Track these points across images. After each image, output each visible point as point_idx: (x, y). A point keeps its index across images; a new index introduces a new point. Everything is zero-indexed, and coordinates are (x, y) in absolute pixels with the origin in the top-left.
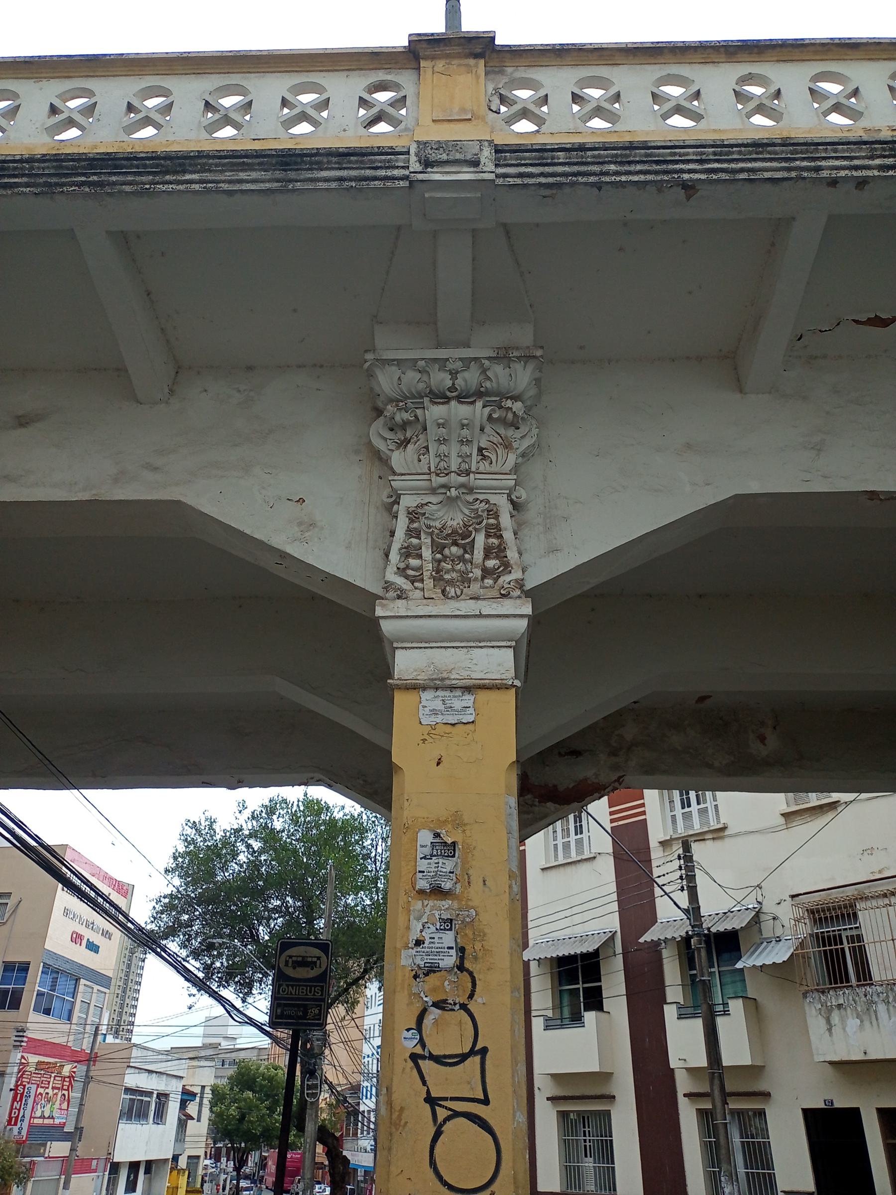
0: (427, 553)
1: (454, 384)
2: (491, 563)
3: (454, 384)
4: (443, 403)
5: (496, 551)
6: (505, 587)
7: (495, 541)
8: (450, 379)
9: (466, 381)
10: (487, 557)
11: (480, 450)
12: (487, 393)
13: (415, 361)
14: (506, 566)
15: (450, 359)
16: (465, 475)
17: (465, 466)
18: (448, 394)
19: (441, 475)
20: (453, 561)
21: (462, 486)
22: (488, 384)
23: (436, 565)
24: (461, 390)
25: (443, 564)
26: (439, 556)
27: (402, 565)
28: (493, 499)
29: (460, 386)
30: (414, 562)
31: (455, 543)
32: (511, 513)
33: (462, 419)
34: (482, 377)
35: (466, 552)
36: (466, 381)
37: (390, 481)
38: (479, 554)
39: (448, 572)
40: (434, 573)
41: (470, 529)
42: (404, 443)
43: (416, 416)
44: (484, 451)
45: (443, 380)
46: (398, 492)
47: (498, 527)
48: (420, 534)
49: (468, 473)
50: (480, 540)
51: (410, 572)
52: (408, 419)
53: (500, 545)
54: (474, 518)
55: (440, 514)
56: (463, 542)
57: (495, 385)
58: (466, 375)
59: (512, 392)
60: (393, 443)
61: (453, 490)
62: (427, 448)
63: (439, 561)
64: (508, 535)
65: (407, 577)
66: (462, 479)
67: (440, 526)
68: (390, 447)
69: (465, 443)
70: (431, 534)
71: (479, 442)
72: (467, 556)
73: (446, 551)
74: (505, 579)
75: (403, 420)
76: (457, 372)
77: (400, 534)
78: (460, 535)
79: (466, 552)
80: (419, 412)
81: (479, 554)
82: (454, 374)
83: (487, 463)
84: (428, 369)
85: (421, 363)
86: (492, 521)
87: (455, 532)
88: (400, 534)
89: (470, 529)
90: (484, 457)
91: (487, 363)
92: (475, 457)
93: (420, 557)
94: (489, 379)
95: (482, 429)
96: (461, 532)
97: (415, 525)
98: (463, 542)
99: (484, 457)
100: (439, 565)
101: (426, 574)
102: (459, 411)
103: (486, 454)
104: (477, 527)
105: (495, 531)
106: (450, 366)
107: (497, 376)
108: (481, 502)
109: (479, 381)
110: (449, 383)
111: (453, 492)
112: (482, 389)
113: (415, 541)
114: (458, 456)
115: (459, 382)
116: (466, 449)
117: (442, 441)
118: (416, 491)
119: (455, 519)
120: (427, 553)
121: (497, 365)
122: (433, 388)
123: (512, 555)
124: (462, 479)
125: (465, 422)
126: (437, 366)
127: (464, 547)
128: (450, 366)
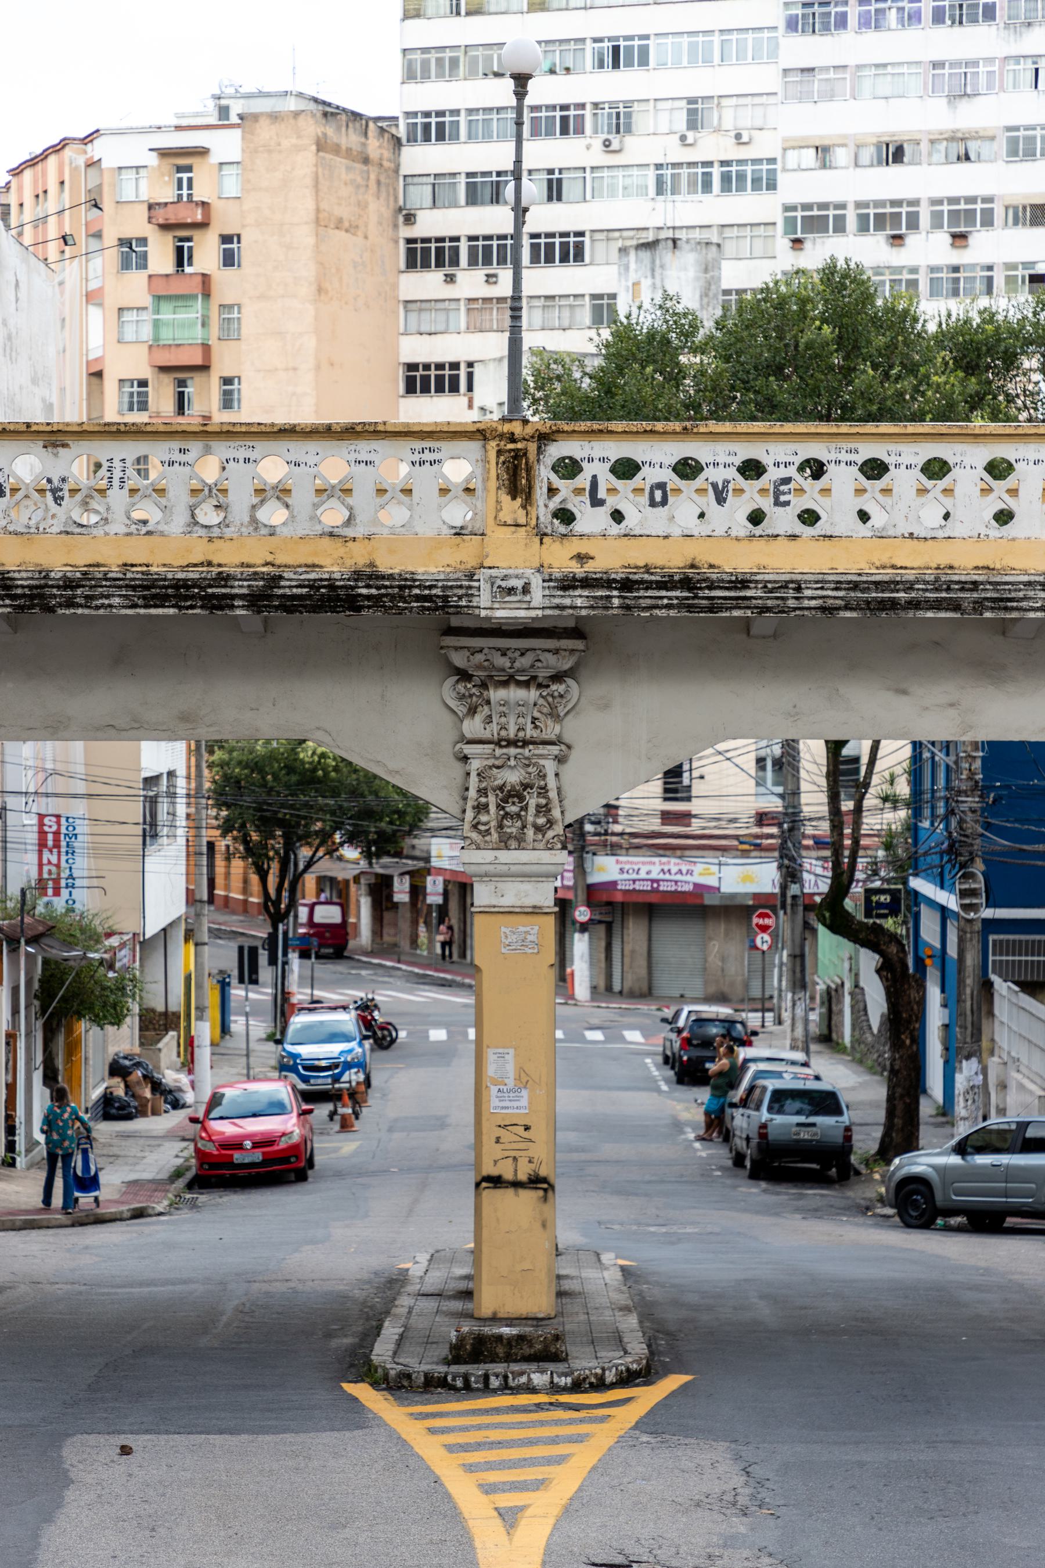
0: (492, 808)
2: (541, 821)
5: (544, 809)
7: (543, 801)
10: (537, 816)
11: (534, 720)
14: (551, 823)
17: (521, 734)
28: (542, 762)
30: (484, 818)
31: (514, 803)
38: (532, 810)
42: (472, 711)
47: (544, 788)
49: (526, 743)
50: (533, 802)
51: (482, 828)
62: (490, 716)
64: (553, 794)
65: (480, 832)
74: (550, 834)
77: (472, 793)
81: (532, 810)
82: (513, 661)
86: (542, 783)
88: (472, 793)
90: (536, 727)
92: (529, 726)
93: (488, 812)
97: (484, 785)
101: (492, 830)
102: (515, 694)
105: (543, 791)
113: (483, 800)
115: (517, 665)
117: (504, 715)
118: (480, 756)
119: (512, 777)
120: (492, 808)
123: (556, 813)
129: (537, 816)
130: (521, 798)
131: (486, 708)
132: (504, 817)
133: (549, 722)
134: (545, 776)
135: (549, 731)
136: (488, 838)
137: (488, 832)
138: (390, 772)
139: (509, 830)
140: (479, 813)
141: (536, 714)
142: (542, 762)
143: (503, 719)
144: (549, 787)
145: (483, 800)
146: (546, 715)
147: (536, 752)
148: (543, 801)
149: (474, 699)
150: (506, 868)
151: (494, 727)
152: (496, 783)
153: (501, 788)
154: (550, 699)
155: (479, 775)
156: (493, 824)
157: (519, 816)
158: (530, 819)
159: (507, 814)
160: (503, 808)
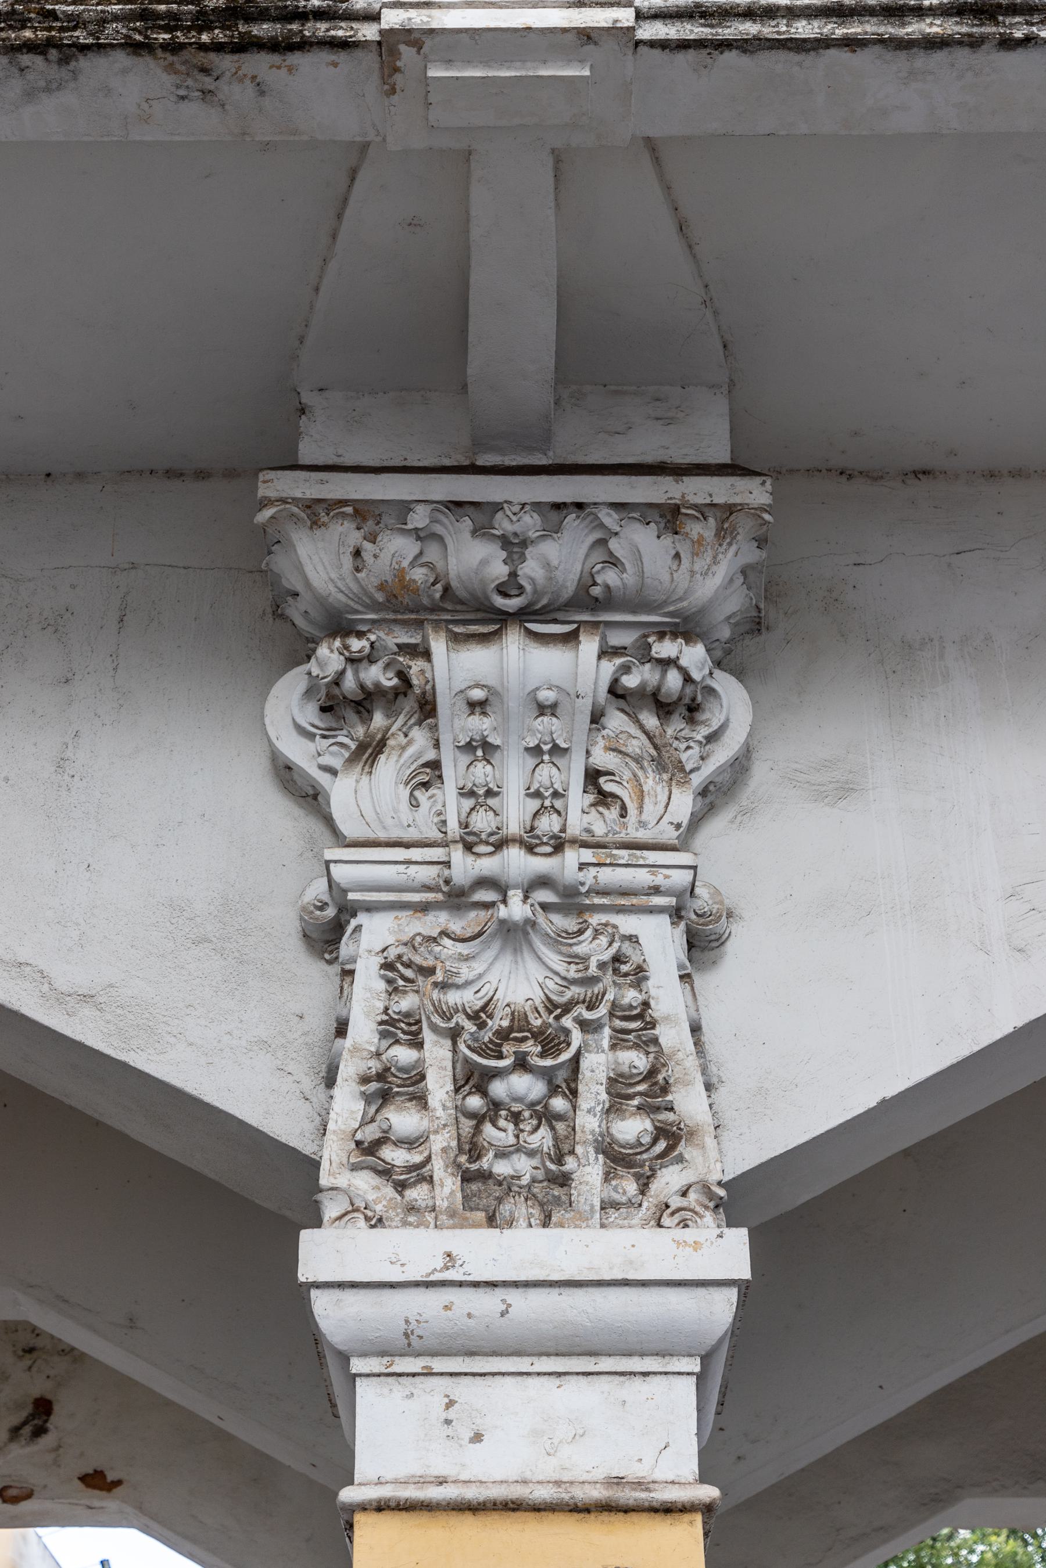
1: (513, 575)
3: (513, 575)
4: (484, 639)
6: (673, 1207)
7: (637, 1060)
8: (505, 562)
9: (547, 565)
10: (615, 1106)
11: (593, 776)
12: (608, 601)
13: (405, 507)
15: (505, 505)
16: (548, 849)
17: (548, 824)
18: (499, 601)
19: (482, 849)
20: (516, 1118)
21: (543, 882)
22: (610, 577)
23: (467, 1125)
24: (535, 591)
25: (488, 1129)
26: (475, 1102)
27: (370, 1133)
29: (532, 580)
31: (522, 1064)
32: (681, 967)
33: (537, 689)
34: (598, 556)
35: (554, 1090)
36: (547, 565)
37: (327, 863)
39: (502, 1154)
40: (463, 1159)
41: (567, 1022)
43: (403, 676)
44: (602, 780)
45: (484, 562)
46: (351, 896)
47: (643, 1013)
48: (420, 1031)
51: (396, 1156)
52: (377, 685)
53: (652, 1072)
54: (574, 982)
55: (478, 967)
56: (548, 1062)
57: (630, 578)
58: (550, 549)
59: (681, 599)
60: (335, 748)
61: (515, 897)
62: (435, 765)
63: (479, 1119)
65: (385, 1172)
66: (540, 865)
67: (480, 1004)
68: (327, 760)
69: (546, 757)
70: (454, 1034)
71: (588, 753)
72: (559, 1104)
73: (498, 1089)
75: (362, 687)
76: (524, 543)
78: (537, 1035)
79: (554, 1090)
80: (416, 667)
83: (612, 814)
84: (438, 529)
85: (419, 518)
86: (631, 996)
87: (519, 1023)
89: (567, 1022)
90: (604, 799)
91: (609, 519)
92: (577, 799)
93: (421, 1100)
94: (613, 562)
95: (597, 718)
96: (538, 1022)
97: (406, 1003)
98: (548, 1062)
99: (604, 799)
100: (477, 1130)
101: (438, 1168)
103: (609, 787)
104: (588, 1015)
106: (503, 524)
107: (638, 556)
108: (597, 933)
109: (588, 566)
110: (499, 570)
111: (516, 909)
112: (596, 591)
113: (403, 1055)
114: (528, 795)
115: (531, 569)
116: (547, 774)
121: (637, 526)
122: (454, 584)
124: (540, 865)
125: (547, 696)
126: (467, 524)
127: (547, 1074)
128: (503, 524)
129: (615, 1106)
130: (551, 1044)
131: (420, 737)
132: (479, 1119)
133: (651, 781)
134: (639, 976)
135: (651, 811)
136: (417, 1194)
137: (420, 1173)
138: (60, 998)
139: (502, 1168)
140: (385, 1097)
141: (602, 759)
142: (627, 924)
143: (481, 773)
144: (658, 1010)
145: (403, 1055)
146: (638, 760)
147: (608, 876)
148: (637, 1060)
149: (379, 720)
150: (487, 1303)
151: (454, 808)
152: (453, 998)
153: (479, 1016)
154: (651, 721)
155: (388, 966)
156: (440, 1142)
157: (545, 1116)
158: (588, 1122)
159: (496, 1106)
160: (482, 1090)
